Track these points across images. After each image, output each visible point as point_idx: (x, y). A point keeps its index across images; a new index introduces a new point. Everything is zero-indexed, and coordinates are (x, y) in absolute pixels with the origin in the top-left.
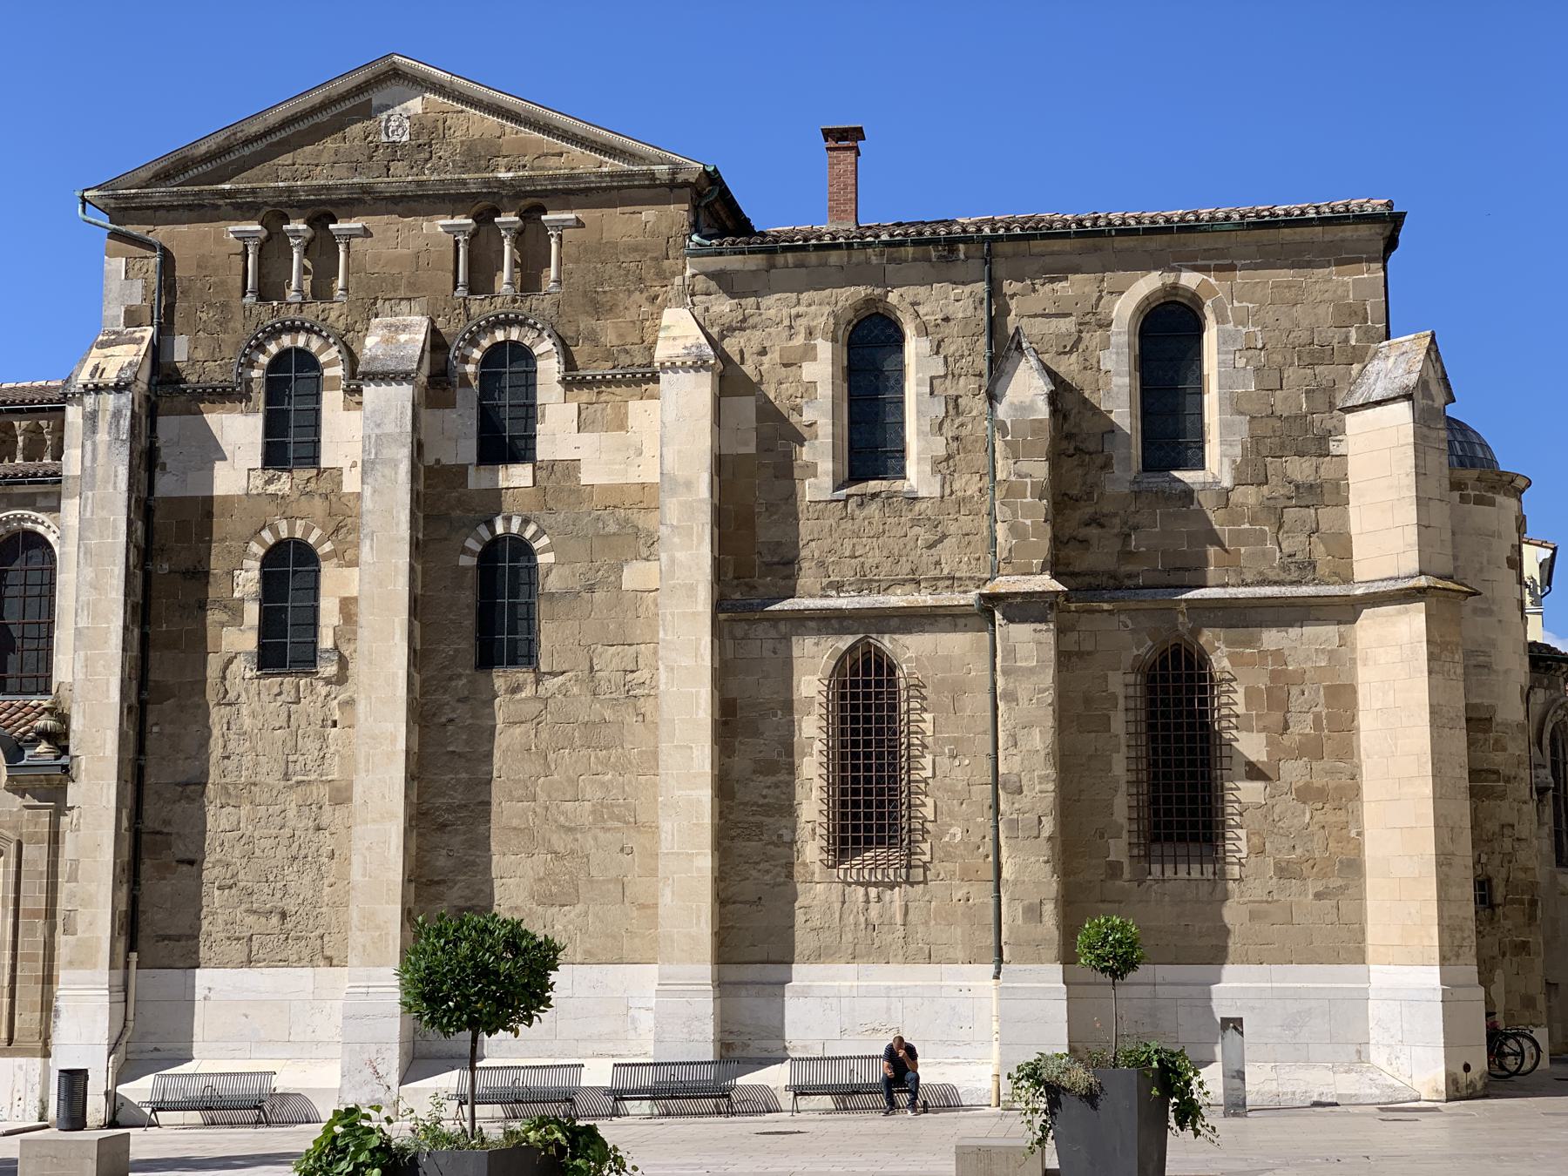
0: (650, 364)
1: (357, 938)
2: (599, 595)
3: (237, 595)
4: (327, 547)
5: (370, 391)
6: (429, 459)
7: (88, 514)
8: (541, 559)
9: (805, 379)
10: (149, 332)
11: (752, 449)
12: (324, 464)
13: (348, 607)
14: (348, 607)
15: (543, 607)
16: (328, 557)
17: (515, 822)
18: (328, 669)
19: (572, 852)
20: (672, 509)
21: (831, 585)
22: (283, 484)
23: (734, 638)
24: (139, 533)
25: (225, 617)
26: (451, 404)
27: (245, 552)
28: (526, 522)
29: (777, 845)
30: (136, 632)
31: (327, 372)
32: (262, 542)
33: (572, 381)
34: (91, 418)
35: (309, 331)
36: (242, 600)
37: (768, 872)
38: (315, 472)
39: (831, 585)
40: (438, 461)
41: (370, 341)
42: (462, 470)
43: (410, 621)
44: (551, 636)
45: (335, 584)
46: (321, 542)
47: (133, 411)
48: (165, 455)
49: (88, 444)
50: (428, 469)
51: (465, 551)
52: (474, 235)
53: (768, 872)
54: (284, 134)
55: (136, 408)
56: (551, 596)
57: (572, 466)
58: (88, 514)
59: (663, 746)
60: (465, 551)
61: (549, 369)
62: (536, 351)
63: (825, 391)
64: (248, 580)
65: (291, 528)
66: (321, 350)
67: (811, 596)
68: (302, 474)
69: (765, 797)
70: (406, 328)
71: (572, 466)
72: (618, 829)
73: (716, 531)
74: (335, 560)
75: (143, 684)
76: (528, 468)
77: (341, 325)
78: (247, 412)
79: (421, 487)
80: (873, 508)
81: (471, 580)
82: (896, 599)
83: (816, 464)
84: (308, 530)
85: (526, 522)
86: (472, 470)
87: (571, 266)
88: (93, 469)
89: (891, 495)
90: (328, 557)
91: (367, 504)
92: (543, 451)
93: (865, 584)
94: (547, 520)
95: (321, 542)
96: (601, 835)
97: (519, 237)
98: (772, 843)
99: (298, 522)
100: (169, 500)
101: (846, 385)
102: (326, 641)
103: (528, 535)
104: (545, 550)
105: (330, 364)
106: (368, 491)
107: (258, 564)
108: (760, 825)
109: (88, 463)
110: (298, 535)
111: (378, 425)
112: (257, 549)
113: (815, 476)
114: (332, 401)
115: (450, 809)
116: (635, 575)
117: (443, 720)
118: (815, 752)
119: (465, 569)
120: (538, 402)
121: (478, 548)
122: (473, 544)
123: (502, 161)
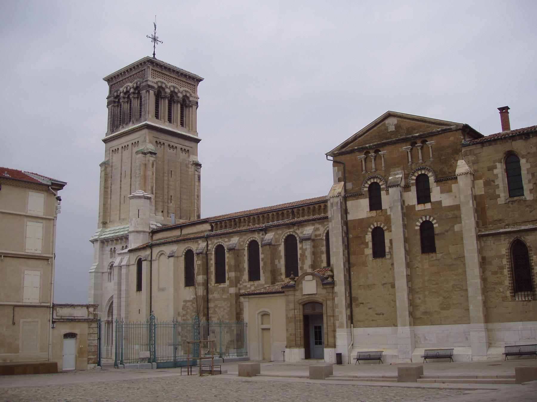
0: (455, 175)
1: (399, 320)
2: (450, 233)
3: (366, 241)
4: (385, 228)
5: (390, 190)
6: (406, 205)
7: (333, 226)
8: (435, 226)
9: (495, 173)
10: (343, 183)
11: (483, 193)
12: (383, 209)
13: (391, 241)
14: (391, 241)
15: (436, 237)
16: (386, 230)
17: (433, 290)
18: (388, 257)
19: (448, 297)
20: (463, 210)
21: (507, 225)
22: (374, 213)
23: (483, 241)
24: (345, 229)
25: (365, 246)
26: (410, 191)
27: (367, 231)
28: (430, 217)
29: (499, 293)
30: (346, 251)
31: (382, 187)
32: (371, 228)
33: (437, 181)
34: (332, 204)
35: (377, 177)
36: (368, 242)
37: (497, 299)
38: (381, 210)
39: (507, 225)
40: (408, 205)
41: (390, 178)
42: (414, 206)
43: (405, 244)
44: (438, 243)
45: (387, 236)
46: (384, 227)
47: (341, 202)
48: (349, 211)
49: (332, 210)
50: (406, 207)
51: (417, 226)
52: (412, 149)
53: (497, 299)
54: (367, 133)
55: (342, 201)
56: (437, 234)
57: (440, 203)
58: (333, 226)
59: (467, 269)
60: (417, 226)
61: (432, 179)
62: (428, 175)
63: (500, 176)
64: (369, 237)
65: (377, 224)
66: (380, 182)
67: (502, 228)
68: (379, 211)
69: (495, 281)
70: (397, 174)
71: (440, 203)
72: (459, 291)
73: (476, 215)
74: (387, 231)
75: (349, 263)
76: (430, 204)
77: (383, 175)
78: (365, 198)
79: (405, 211)
80: (515, 204)
81: (418, 233)
82: (523, 228)
83: (500, 195)
84: (381, 224)
85: (430, 217)
86: (416, 206)
87: (434, 153)
88: (333, 215)
89: (520, 200)
90: (386, 230)
91: (392, 217)
92: (433, 199)
93: (515, 224)
94: (435, 216)
95: (384, 227)
96: (455, 292)
97: (422, 148)
98: (498, 292)
99: (379, 223)
100: (351, 220)
101: (506, 174)
102: (387, 250)
103: (431, 220)
104: (435, 223)
105: (382, 185)
106: (392, 214)
107: (371, 233)
108: (494, 288)
109: (332, 214)
110: (379, 226)
111: (393, 198)
112: (370, 230)
113: (500, 198)
114: (383, 193)
115: (419, 288)
116: (457, 228)
117: (415, 267)
118: (506, 268)
119: (417, 230)
120: (430, 188)
121: (419, 224)
122: (419, 224)
123: (416, 131)
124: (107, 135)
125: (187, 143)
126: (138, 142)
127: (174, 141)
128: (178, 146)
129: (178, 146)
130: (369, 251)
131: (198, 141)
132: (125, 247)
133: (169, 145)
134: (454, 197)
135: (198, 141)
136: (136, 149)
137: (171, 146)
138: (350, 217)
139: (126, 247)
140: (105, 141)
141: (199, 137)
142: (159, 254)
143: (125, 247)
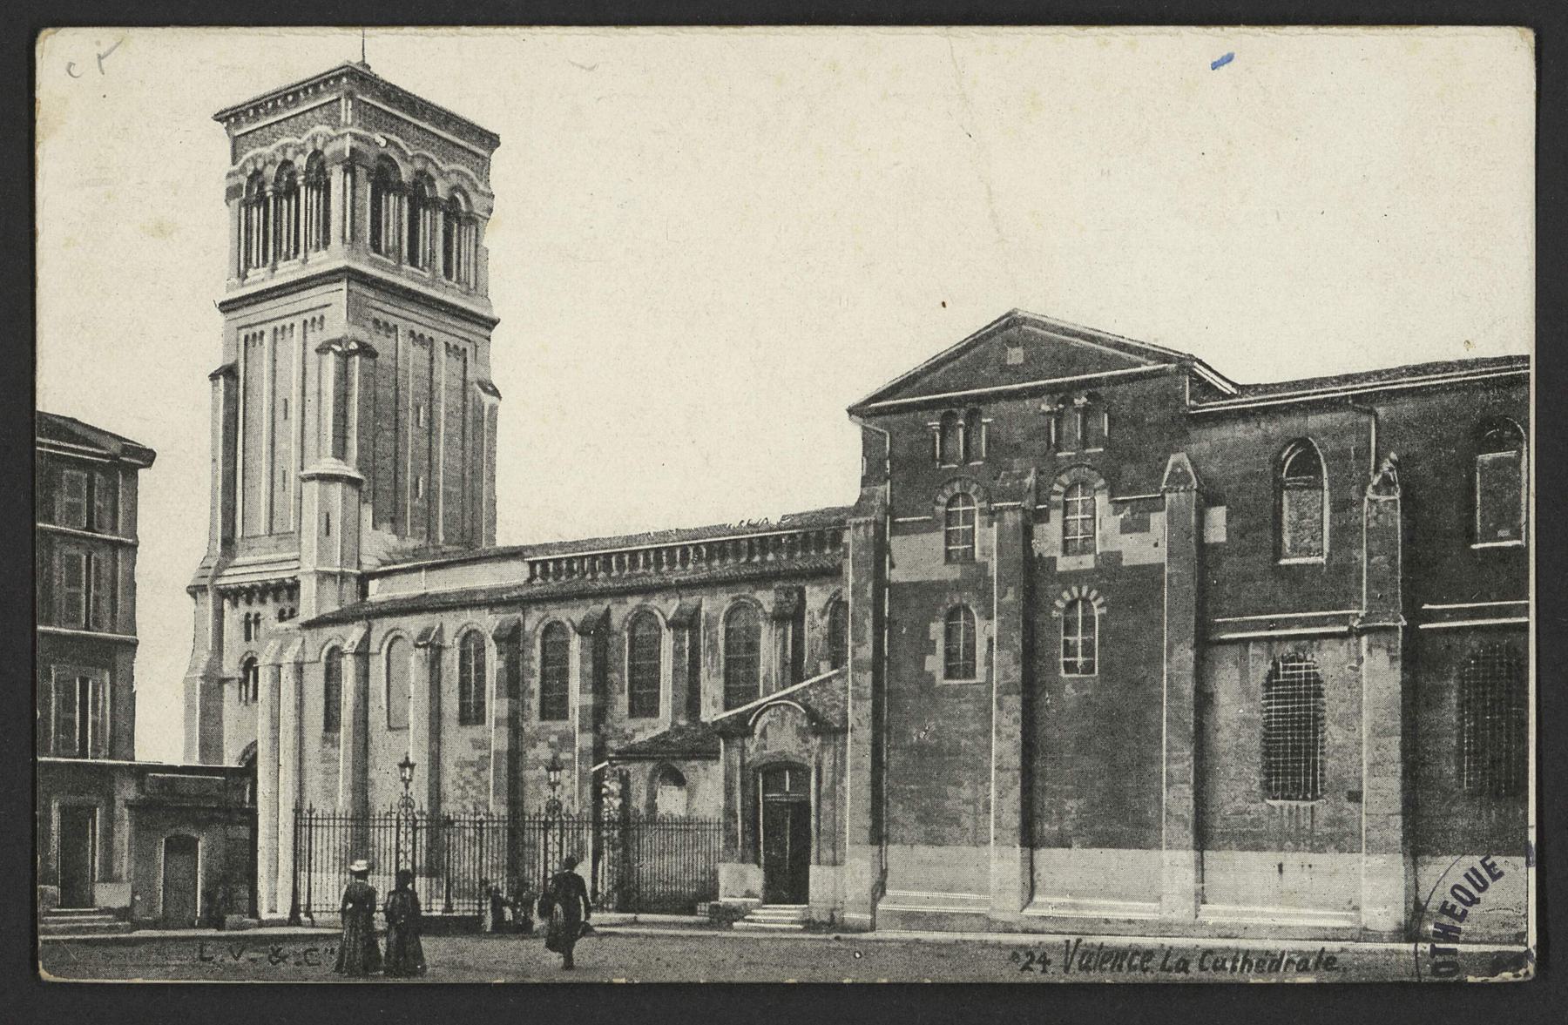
124: (229, 289)
125: (462, 328)
126: (322, 318)
127: (422, 321)
128: (434, 334)
129: (434, 334)
130: (935, 664)
131: (491, 323)
132: (287, 614)
133: (412, 333)
134: (1152, 546)
135: (491, 323)
136: (315, 340)
137: (417, 334)
138: (896, 575)
139: (293, 613)
140: (227, 307)
141: (495, 314)
142: (390, 637)
143: (287, 614)
